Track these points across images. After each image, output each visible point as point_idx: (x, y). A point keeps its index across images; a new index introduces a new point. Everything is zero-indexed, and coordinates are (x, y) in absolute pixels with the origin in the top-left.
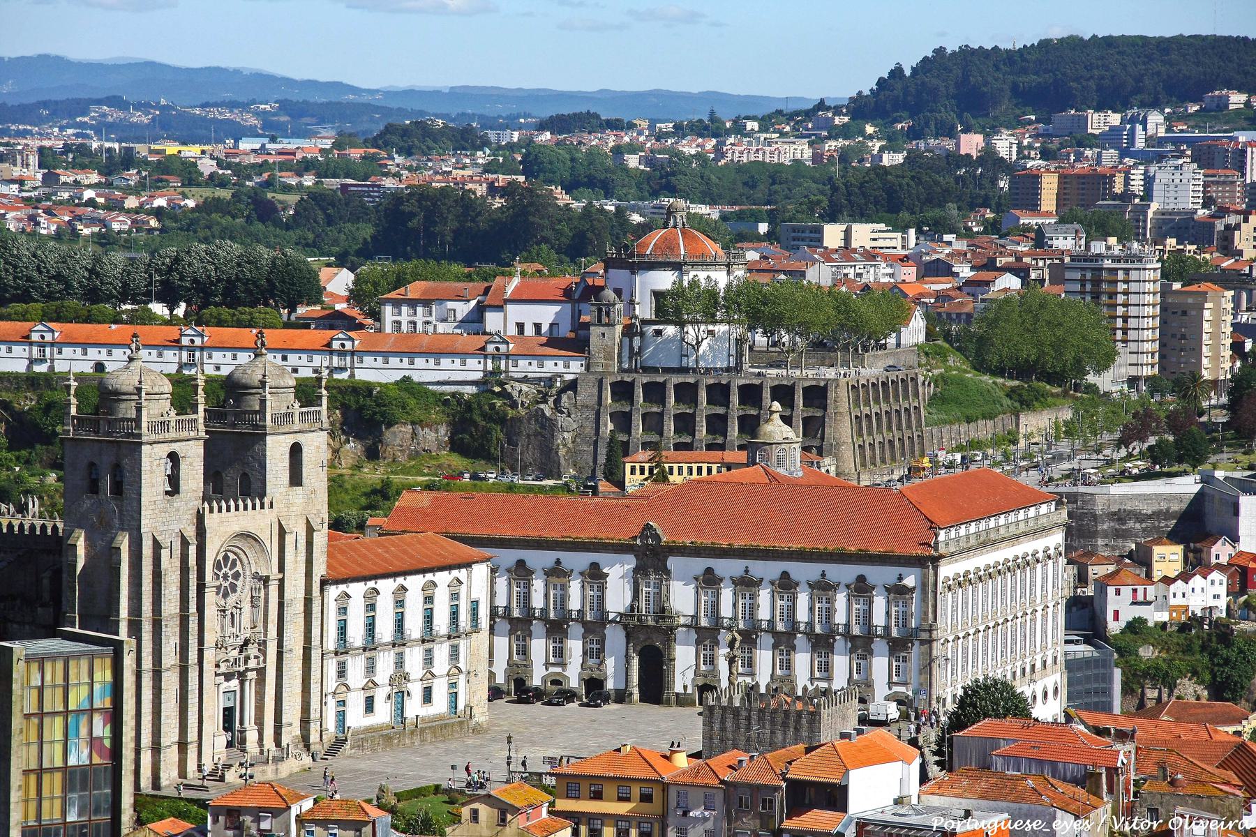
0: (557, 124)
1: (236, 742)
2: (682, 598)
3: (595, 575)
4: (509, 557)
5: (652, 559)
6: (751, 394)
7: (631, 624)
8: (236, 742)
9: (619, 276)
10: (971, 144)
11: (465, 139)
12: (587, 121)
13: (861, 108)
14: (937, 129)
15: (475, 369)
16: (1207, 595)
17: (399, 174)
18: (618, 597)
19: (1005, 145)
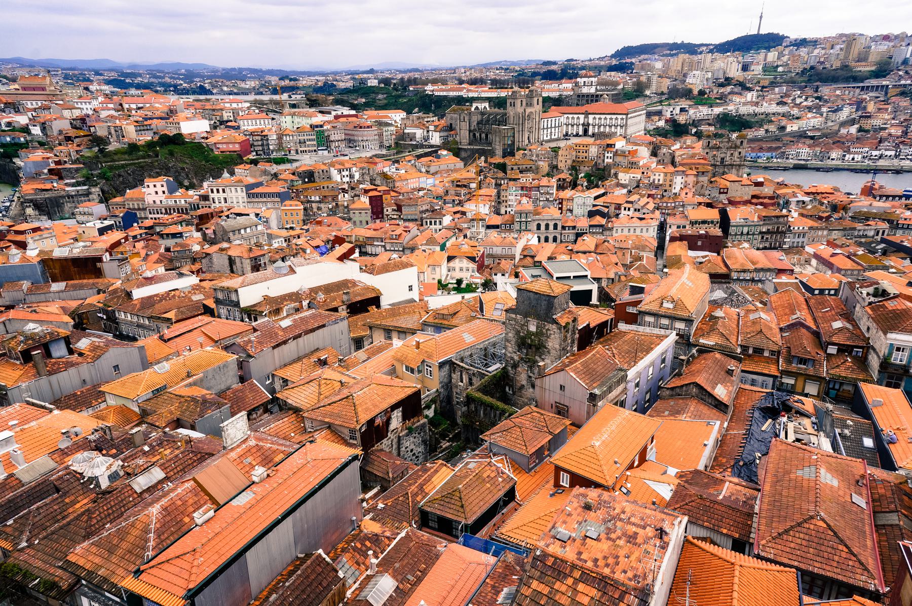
0: (567, 61)
1: (529, 142)
2: (591, 121)
3: (578, 118)
4: (566, 116)
5: (587, 114)
6: (597, 96)
7: (583, 125)
8: (529, 142)
9: (578, 79)
10: (629, 61)
11: (555, 63)
12: (572, 60)
13: (613, 56)
14: (623, 60)
15: (558, 94)
16: (662, 124)
17: (545, 69)
18: (582, 121)
19: (633, 60)
